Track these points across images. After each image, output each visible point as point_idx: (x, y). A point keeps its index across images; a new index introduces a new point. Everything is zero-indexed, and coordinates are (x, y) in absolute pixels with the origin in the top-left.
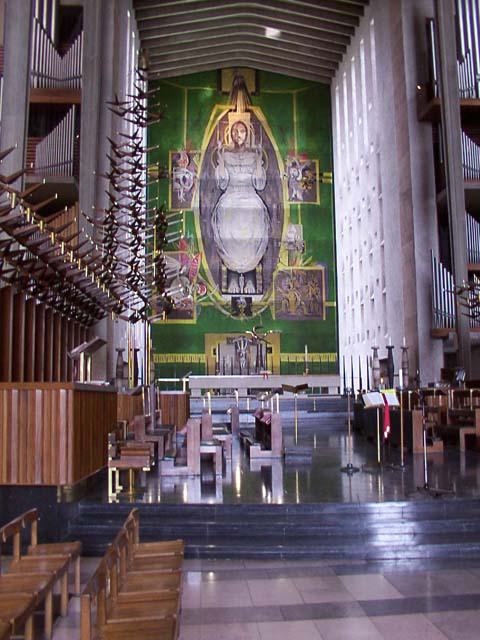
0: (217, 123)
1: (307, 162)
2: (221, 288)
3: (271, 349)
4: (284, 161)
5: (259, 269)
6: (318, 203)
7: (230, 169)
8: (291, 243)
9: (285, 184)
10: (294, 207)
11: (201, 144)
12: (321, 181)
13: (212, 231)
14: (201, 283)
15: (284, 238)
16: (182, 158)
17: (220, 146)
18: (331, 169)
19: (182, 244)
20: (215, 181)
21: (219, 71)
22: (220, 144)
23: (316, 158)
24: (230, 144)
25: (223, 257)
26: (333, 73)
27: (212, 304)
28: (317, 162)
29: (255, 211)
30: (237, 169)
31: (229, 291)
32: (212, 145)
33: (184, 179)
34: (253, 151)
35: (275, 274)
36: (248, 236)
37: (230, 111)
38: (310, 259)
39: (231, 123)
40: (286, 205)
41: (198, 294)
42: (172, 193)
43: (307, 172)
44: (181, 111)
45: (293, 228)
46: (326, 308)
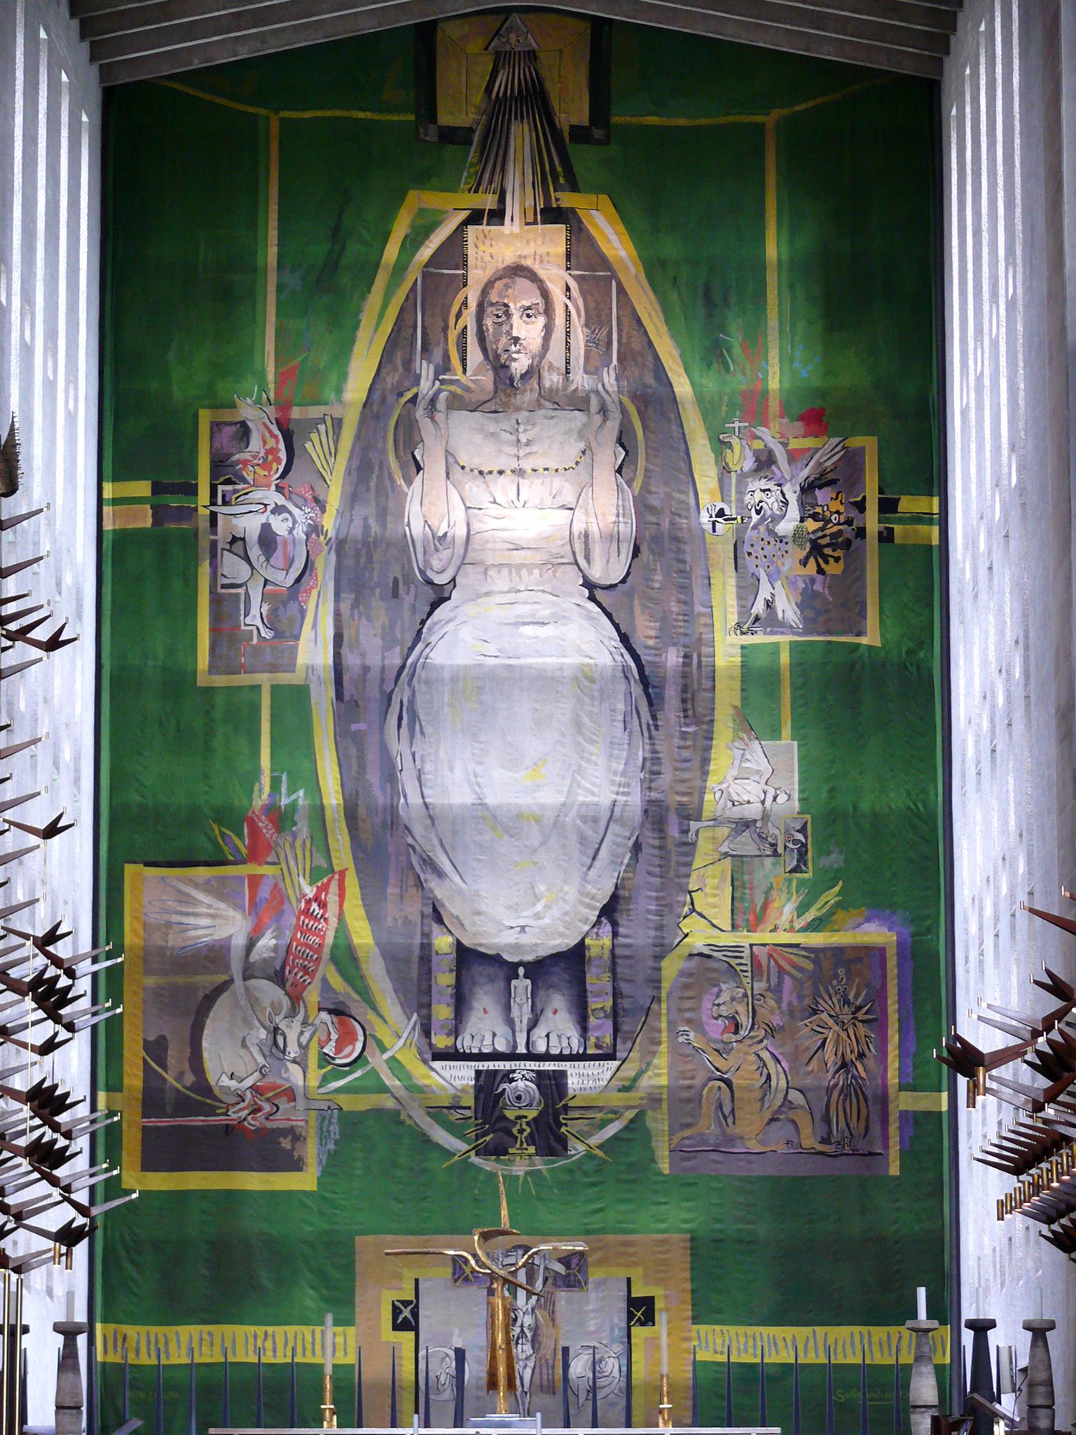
0: (413, 274)
1: (825, 450)
2: (427, 1032)
3: (648, 1303)
4: (720, 446)
5: (600, 943)
6: (871, 638)
7: (475, 489)
8: (745, 825)
10: (760, 661)
11: (344, 376)
12: (886, 537)
13: (391, 776)
14: (339, 1012)
15: (712, 802)
16: (255, 444)
17: (426, 386)
19: (255, 832)
20: (403, 546)
21: (426, 34)
22: (426, 371)
25: (439, 890)
26: (939, 65)
27: (390, 1103)
28: (867, 444)
29: (585, 679)
30: (504, 488)
31: (466, 1043)
32: (390, 380)
33: (267, 539)
34: (579, 403)
35: (671, 968)
36: (549, 797)
37: (475, 217)
38: (831, 896)
39: (477, 275)
41: (325, 1059)
42: (216, 600)
43: (822, 496)
44: (253, 221)
45: (757, 756)
46: (904, 1115)
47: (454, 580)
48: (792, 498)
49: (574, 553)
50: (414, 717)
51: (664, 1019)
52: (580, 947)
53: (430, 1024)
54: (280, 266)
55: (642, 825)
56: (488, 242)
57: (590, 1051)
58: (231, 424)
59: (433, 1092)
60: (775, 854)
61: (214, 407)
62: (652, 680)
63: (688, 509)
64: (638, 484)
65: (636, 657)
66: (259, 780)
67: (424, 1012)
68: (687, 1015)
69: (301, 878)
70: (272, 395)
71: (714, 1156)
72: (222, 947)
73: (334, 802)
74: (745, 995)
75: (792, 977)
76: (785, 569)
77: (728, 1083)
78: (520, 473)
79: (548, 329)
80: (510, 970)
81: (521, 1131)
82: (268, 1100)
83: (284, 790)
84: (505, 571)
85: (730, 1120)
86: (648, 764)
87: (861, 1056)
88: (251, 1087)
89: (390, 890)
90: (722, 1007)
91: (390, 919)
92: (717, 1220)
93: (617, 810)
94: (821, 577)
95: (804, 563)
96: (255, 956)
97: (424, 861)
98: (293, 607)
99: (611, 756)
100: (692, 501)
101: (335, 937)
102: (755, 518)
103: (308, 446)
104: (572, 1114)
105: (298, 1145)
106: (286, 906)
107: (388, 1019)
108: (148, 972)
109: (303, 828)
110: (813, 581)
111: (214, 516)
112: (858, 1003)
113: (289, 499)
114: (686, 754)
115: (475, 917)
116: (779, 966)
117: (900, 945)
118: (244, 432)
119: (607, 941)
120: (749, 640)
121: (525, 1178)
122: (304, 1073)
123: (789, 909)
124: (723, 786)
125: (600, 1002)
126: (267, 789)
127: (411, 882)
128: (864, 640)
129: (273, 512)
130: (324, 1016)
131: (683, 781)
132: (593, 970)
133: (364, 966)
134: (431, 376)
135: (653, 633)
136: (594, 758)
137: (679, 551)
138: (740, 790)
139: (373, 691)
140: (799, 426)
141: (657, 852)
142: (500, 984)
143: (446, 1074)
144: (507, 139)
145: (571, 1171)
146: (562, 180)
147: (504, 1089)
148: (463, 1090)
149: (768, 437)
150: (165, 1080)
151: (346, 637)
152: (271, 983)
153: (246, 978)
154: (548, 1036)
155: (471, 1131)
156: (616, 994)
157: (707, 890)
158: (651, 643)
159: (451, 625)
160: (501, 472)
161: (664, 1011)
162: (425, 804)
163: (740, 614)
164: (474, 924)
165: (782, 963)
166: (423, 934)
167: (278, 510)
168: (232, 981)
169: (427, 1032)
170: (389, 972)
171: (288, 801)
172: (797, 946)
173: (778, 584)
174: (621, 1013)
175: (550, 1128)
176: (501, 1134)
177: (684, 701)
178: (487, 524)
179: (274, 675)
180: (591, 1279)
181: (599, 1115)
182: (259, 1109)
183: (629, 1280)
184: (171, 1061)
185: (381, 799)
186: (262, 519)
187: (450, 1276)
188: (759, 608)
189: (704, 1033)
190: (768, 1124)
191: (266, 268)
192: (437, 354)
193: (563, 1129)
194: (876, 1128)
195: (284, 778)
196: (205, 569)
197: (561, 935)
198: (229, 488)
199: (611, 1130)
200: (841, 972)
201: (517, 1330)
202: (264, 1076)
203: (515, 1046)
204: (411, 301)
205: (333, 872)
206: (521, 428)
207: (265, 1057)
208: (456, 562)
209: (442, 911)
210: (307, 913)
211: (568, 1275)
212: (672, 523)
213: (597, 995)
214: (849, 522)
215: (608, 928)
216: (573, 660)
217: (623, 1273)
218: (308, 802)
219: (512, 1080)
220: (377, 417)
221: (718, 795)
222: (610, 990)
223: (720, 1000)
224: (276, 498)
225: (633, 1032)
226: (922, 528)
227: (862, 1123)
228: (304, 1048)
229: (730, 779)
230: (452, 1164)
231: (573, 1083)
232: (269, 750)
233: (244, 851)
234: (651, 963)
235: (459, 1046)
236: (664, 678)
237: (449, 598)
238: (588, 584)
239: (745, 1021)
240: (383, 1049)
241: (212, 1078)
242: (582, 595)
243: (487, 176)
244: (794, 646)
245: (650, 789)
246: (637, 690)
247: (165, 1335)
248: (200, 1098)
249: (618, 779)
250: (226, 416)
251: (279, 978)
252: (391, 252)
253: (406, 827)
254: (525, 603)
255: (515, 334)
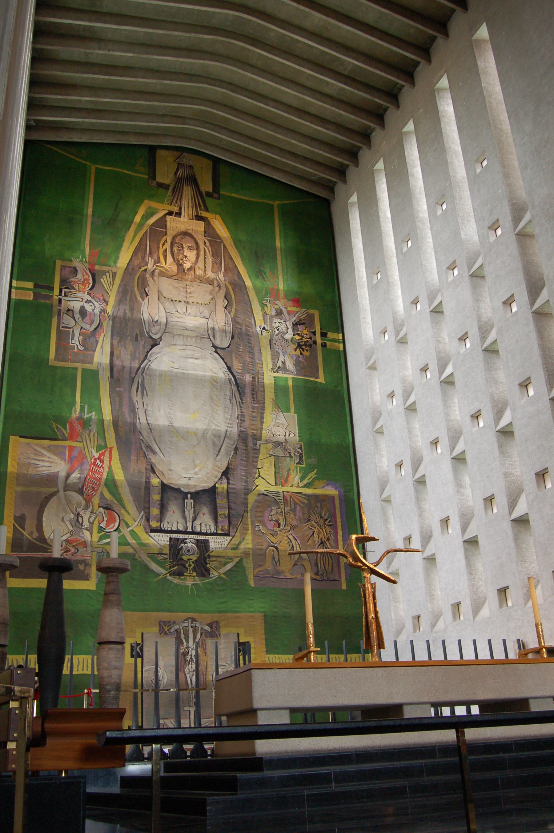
0: (146, 228)
1: (300, 313)
2: (148, 520)
4: (263, 305)
5: (222, 486)
6: (321, 379)
7: (170, 307)
8: (278, 444)
9: (265, 342)
10: (281, 383)
11: (117, 258)
12: (324, 345)
13: (133, 410)
15: (265, 434)
16: (79, 276)
17: (150, 266)
18: (341, 329)
19: (72, 427)
20: (140, 322)
23: (316, 308)
24: (170, 265)
25: (154, 459)
27: (131, 551)
28: (316, 313)
29: (214, 382)
30: (181, 307)
31: (165, 526)
32: (136, 262)
33: (83, 312)
34: (210, 282)
35: (252, 499)
37: (170, 213)
38: (312, 475)
40: (268, 378)
41: (101, 529)
42: (59, 332)
45: (282, 418)
47: (161, 338)
48: (290, 327)
49: (209, 334)
50: (143, 388)
51: (249, 520)
52: (214, 488)
53: (149, 516)
54: (93, 215)
55: (238, 440)
56: (175, 222)
57: (219, 532)
58: (70, 267)
59: (150, 546)
60: (291, 456)
61: (63, 260)
62: (241, 385)
63: (252, 325)
64: (233, 313)
65: (234, 376)
66: (75, 406)
67: (147, 511)
68: (259, 519)
69: (92, 449)
70: (87, 260)
71: (272, 579)
72: (54, 476)
73: (108, 419)
74: (282, 512)
75: (299, 505)
76: (289, 351)
77: (276, 548)
78: (188, 303)
79: (198, 255)
80: (185, 495)
81: (190, 565)
82: (73, 546)
83: (86, 411)
84: (181, 337)
85: (278, 564)
86: (240, 417)
87: (328, 539)
88: (65, 540)
89: (132, 457)
90: (273, 516)
91: (132, 470)
92: (275, 607)
93: (228, 435)
94: (301, 356)
95: (295, 350)
96: (70, 481)
97: (147, 447)
98: (93, 339)
99: (225, 412)
100: (253, 323)
101: (107, 476)
102: (277, 332)
103: (102, 280)
104: (212, 559)
105: (87, 568)
106: (85, 460)
107: (130, 512)
108: (18, 484)
109: (94, 428)
110: (299, 357)
111: (60, 301)
112: (326, 517)
113: (93, 298)
114: (254, 414)
115: (169, 472)
116: (295, 501)
117: (340, 496)
118: (75, 271)
119: (225, 486)
120: (276, 375)
121: (192, 587)
122: (91, 534)
123: (297, 478)
124: (269, 428)
125: (223, 512)
126: (78, 410)
127: (142, 454)
128: (319, 380)
129: (86, 302)
130: (101, 510)
131: (254, 425)
132: (220, 497)
133: (120, 489)
134: (153, 263)
135: (240, 368)
136: (218, 412)
137: (249, 339)
138: (276, 430)
139: (126, 375)
140: (291, 303)
141: (244, 452)
142: (181, 501)
143: (156, 539)
144: (182, 191)
145: (212, 584)
146: (202, 208)
147: (182, 547)
148: (164, 546)
149: (280, 304)
150: (23, 535)
151: (115, 354)
152: (76, 494)
153: (65, 491)
154: (201, 524)
155: (167, 565)
156: (230, 508)
157: (265, 468)
158: (239, 371)
159: (159, 355)
160: (180, 301)
161: (249, 517)
162: (148, 423)
163: (273, 365)
164: (169, 474)
165: (296, 500)
166: (147, 477)
167: (88, 301)
168: (58, 491)
169: (148, 520)
170: (131, 492)
171: (88, 416)
172: (301, 493)
173: (286, 356)
174: (231, 516)
175: (202, 564)
176: (181, 566)
177: (253, 394)
178: (175, 319)
179: (83, 364)
180: (222, 634)
181: (223, 560)
182: (69, 551)
183: (238, 634)
184: (27, 526)
185: (128, 419)
186: (81, 304)
187: (158, 631)
188: (280, 364)
189: (266, 527)
190: (293, 566)
191: (87, 216)
192: (155, 256)
193: (208, 565)
194: (336, 569)
195: (86, 406)
196: (55, 320)
197: (206, 482)
198: (68, 290)
199: (229, 567)
200: (318, 504)
201: (188, 658)
202: (72, 535)
203: (187, 528)
204: (145, 235)
205: (107, 447)
206: (188, 287)
207: (73, 527)
208: (162, 331)
209: (155, 468)
210: (94, 464)
211: (211, 632)
212: (246, 329)
213: (221, 508)
214: (310, 338)
215: (226, 480)
216: (209, 374)
217: (236, 631)
218: (96, 417)
219: (186, 543)
220: (131, 274)
221: (268, 431)
222: (227, 506)
223: (272, 513)
224: (87, 297)
225: (237, 525)
226: (337, 344)
227: (330, 568)
228: (92, 524)
229: (272, 426)
230: (159, 580)
231: (212, 545)
232: (80, 394)
233: (67, 435)
234: (243, 496)
235: (162, 526)
236: (245, 385)
237: (159, 344)
238: (214, 346)
239: (282, 522)
240: (128, 526)
241: (46, 535)
242: (212, 350)
243: (175, 201)
244: (293, 379)
245: (241, 426)
246: (235, 388)
247: (17, 660)
248: (40, 544)
249: (228, 421)
250: (67, 264)
251: (81, 491)
252: (138, 219)
253: (140, 432)
254: (189, 350)
255: (185, 254)
